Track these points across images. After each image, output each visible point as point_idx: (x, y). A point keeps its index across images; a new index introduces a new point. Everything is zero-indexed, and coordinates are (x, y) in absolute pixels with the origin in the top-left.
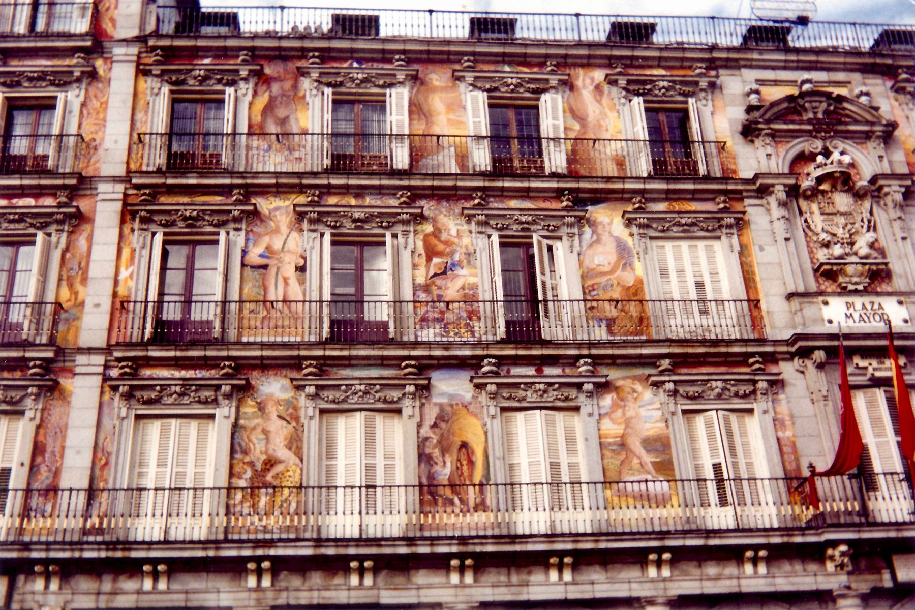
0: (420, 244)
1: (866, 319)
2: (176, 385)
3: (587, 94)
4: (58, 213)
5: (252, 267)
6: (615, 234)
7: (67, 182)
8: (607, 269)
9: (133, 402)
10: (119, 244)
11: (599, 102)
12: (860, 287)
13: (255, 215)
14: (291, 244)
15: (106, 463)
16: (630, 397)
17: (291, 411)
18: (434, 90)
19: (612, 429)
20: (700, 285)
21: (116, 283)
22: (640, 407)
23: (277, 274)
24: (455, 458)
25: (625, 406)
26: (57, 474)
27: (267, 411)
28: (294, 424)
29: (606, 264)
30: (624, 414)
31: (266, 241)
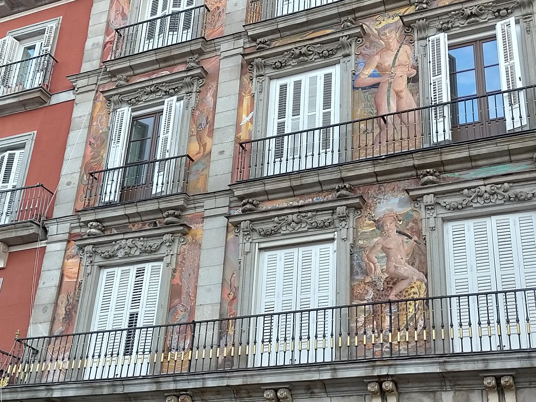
2: (292, 214)
4: (186, 77)
5: (363, 89)
7: (194, 48)
9: (255, 236)
10: (240, 94)
13: (363, 35)
14: (402, 57)
15: (234, 298)
17: (411, 224)
21: (238, 128)
23: (389, 91)
26: (192, 312)
27: (386, 228)
28: (416, 238)
31: (377, 58)
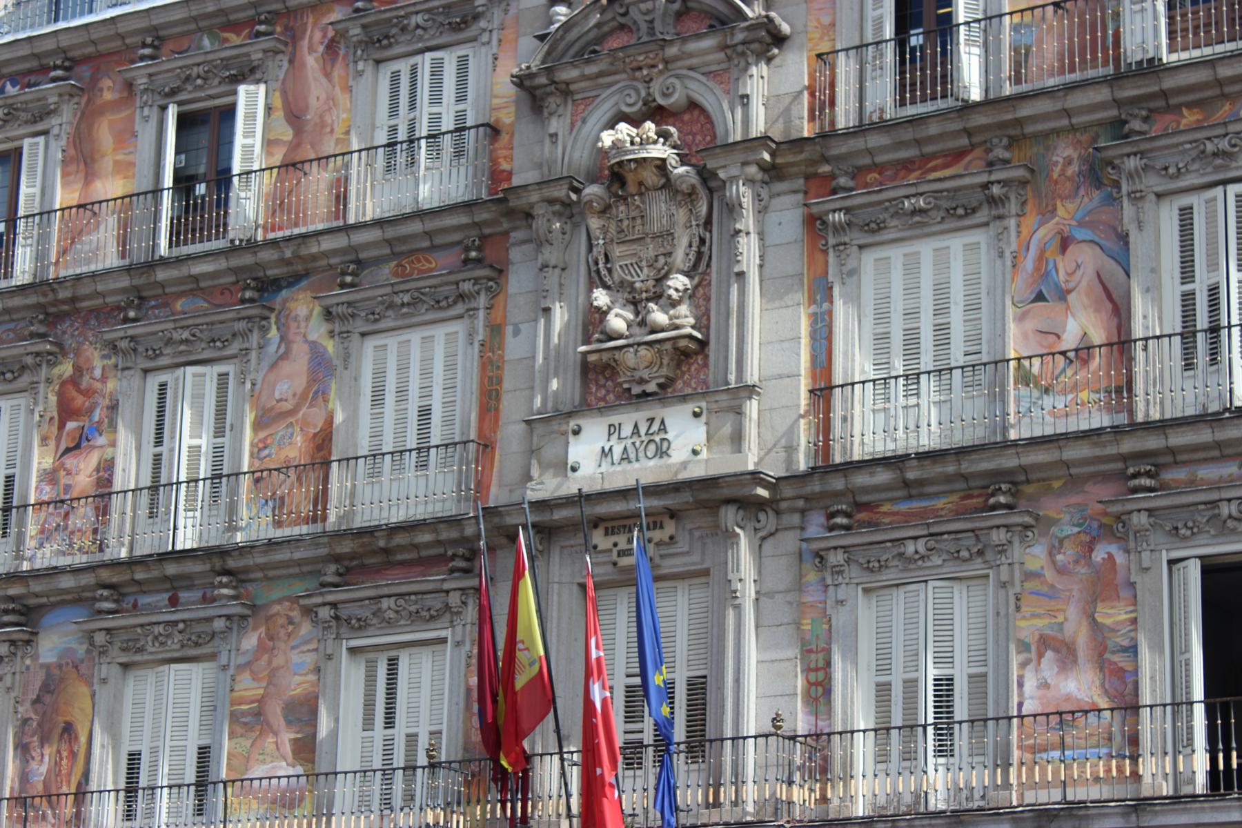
0: (53, 399)
1: (632, 456)
3: (311, 62)
6: (313, 337)
8: (288, 406)
11: (328, 75)
12: (651, 387)
16: (282, 632)
18: (101, 111)
19: (249, 687)
20: (425, 413)
22: (293, 648)
24: (55, 749)
25: (274, 648)
29: (290, 397)
30: (270, 662)
